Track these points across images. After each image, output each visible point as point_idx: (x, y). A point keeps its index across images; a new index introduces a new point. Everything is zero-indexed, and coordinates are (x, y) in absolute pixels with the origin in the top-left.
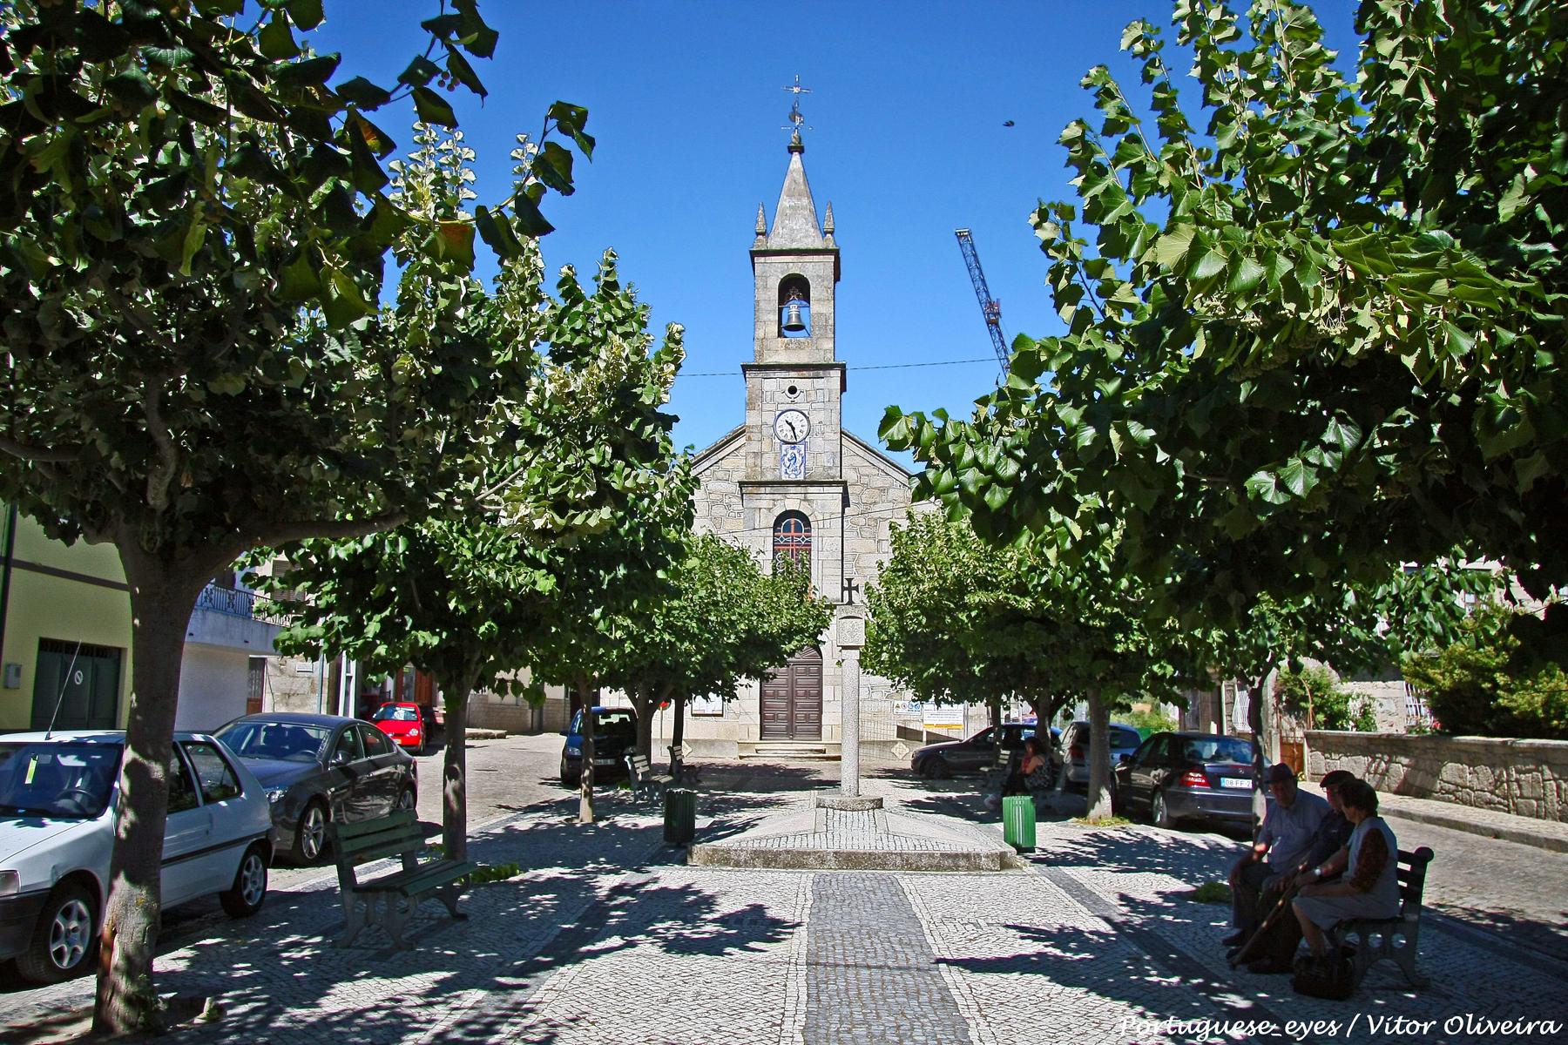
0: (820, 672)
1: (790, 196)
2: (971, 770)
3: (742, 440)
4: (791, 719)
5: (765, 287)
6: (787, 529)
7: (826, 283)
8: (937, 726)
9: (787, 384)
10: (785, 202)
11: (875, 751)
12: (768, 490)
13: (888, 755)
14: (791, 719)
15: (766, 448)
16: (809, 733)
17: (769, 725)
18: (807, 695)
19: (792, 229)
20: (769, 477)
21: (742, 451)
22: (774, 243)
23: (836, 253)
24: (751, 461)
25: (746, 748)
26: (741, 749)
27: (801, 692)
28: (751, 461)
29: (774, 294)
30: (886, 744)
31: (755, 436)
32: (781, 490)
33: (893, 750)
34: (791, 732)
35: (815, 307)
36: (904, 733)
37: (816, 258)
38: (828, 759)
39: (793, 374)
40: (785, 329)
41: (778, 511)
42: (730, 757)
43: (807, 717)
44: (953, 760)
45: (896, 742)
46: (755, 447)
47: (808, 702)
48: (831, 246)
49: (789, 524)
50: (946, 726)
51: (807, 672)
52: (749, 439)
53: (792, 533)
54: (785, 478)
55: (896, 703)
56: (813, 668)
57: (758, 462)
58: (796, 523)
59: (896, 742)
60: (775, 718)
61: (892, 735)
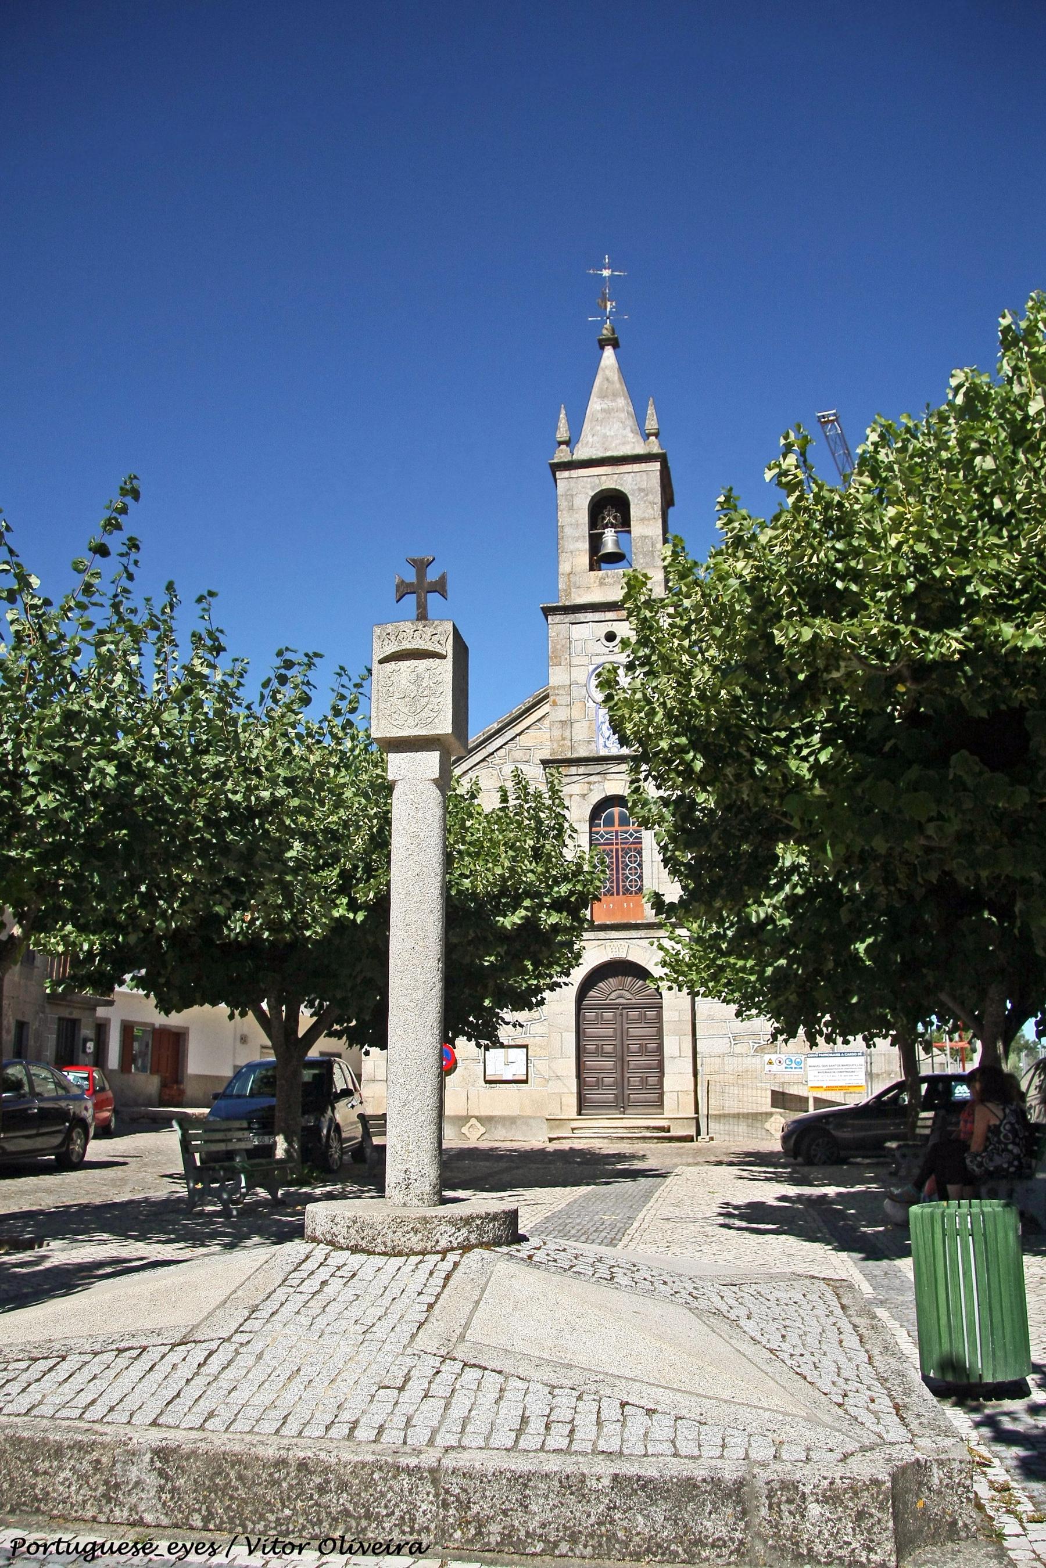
0: (659, 1018)
1: (603, 396)
2: (874, 1148)
3: (545, 709)
4: (621, 1084)
5: (571, 508)
6: (609, 822)
7: (650, 498)
8: (829, 1088)
9: (604, 629)
10: (595, 405)
11: (742, 1128)
12: (582, 770)
13: (761, 1133)
14: (621, 1084)
15: (576, 714)
16: (647, 1104)
17: (593, 1096)
18: (643, 1050)
19: (605, 436)
20: (582, 753)
21: (546, 722)
22: (582, 453)
23: (662, 458)
24: (557, 733)
25: (558, 1127)
26: (551, 1128)
27: (634, 1047)
28: (557, 733)
29: (584, 517)
30: (757, 1118)
31: (563, 700)
32: (599, 768)
33: (767, 1126)
34: (622, 1104)
35: (637, 529)
36: (780, 1099)
37: (636, 467)
38: (671, 1139)
39: (610, 615)
40: (599, 559)
41: (596, 797)
42: (536, 1139)
43: (644, 1081)
44: (844, 1134)
45: (771, 1114)
46: (562, 714)
47: (643, 1060)
48: (656, 449)
49: (611, 815)
50: (841, 1088)
51: (642, 1018)
52: (555, 704)
53: (616, 827)
54: (603, 752)
55: (767, 1058)
56: (651, 1014)
57: (567, 734)
58: (621, 814)
59: (771, 1114)
60: (599, 1084)
61: (765, 1103)
